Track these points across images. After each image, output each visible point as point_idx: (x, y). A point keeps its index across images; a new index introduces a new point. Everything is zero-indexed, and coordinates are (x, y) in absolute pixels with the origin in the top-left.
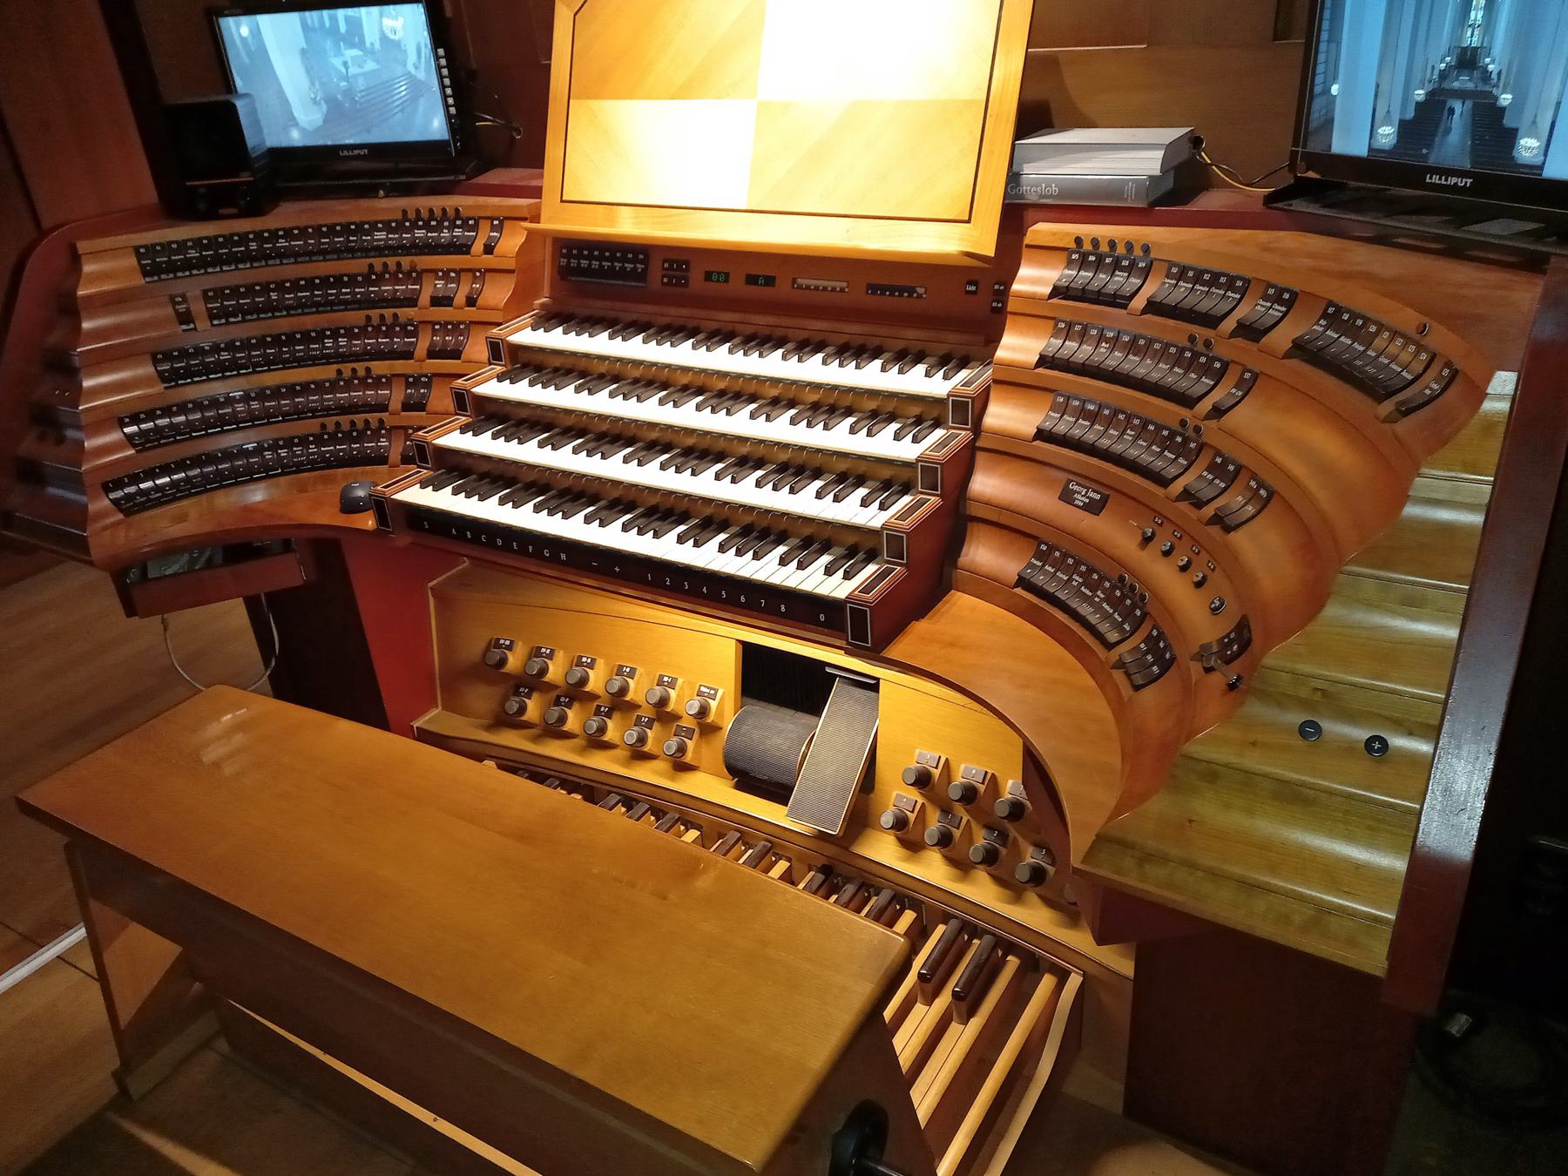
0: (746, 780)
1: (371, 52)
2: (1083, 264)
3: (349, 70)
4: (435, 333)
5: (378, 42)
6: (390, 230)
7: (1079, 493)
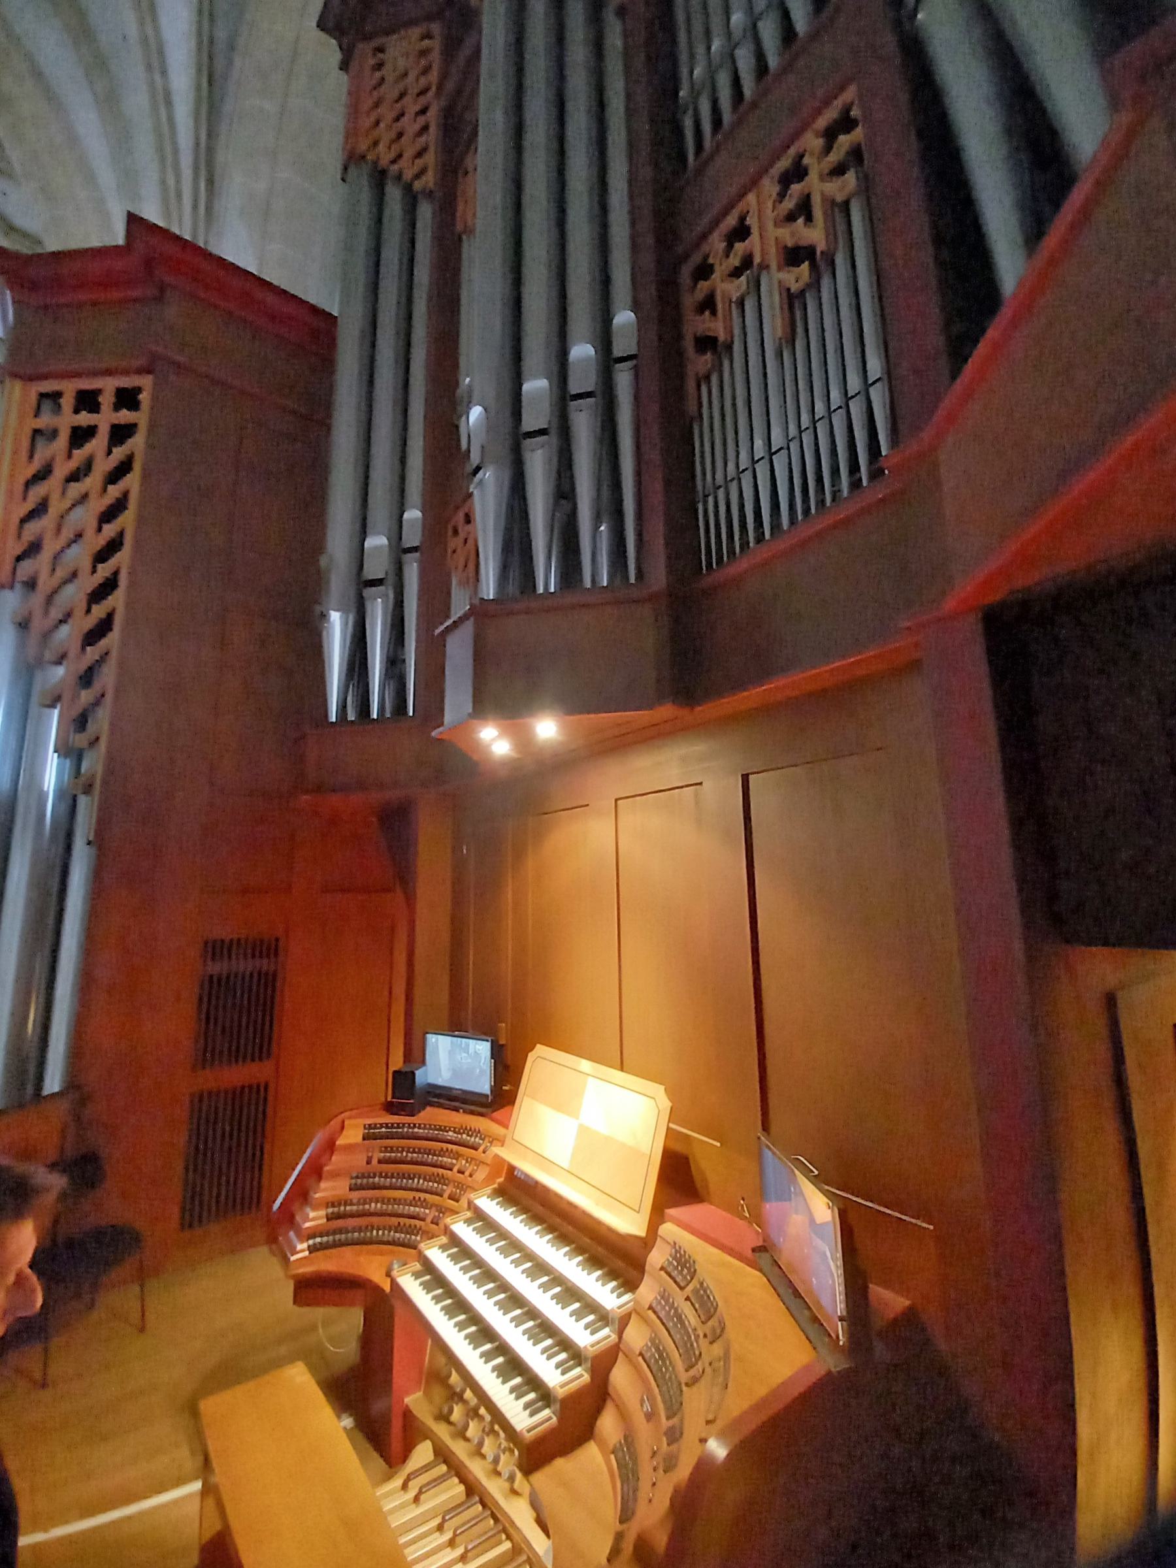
6: (455, 1132)
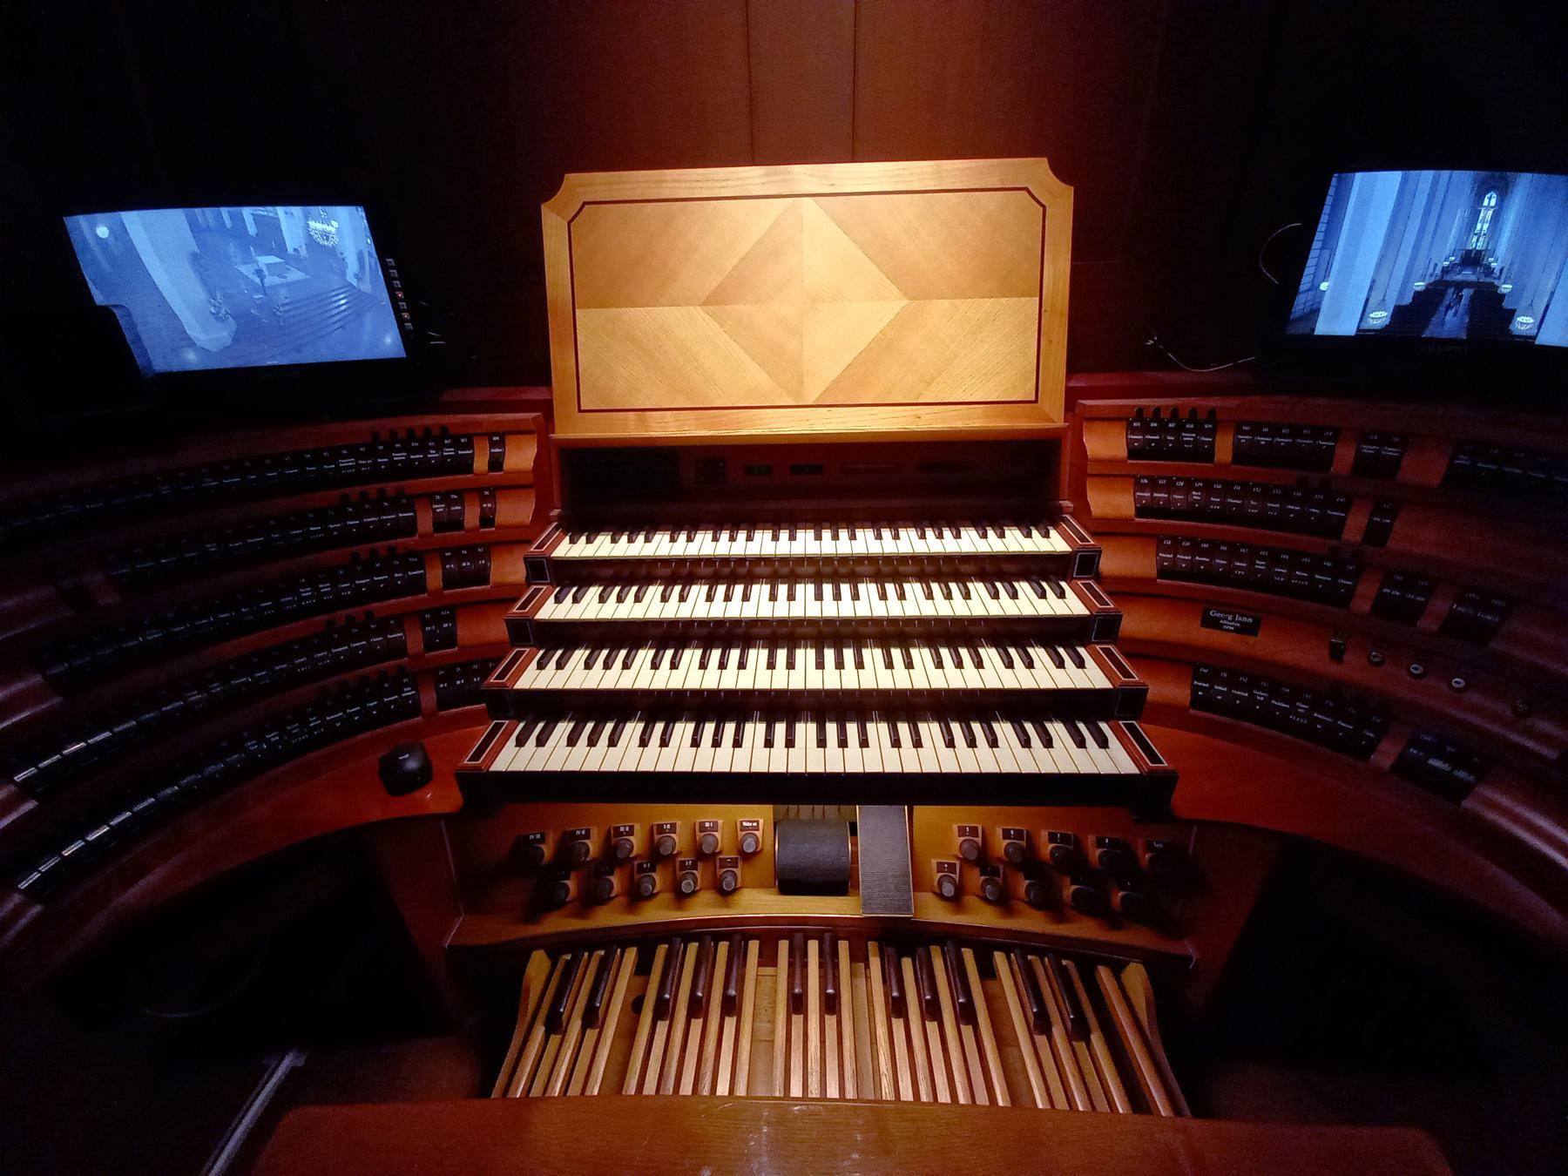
0: (791, 883)
1: (295, 260)
2: (1146, 429)
3: (266, 281)
4: (445, 561)
5: (304, 247)
6: (359, 456)
7: (1226, 619)
